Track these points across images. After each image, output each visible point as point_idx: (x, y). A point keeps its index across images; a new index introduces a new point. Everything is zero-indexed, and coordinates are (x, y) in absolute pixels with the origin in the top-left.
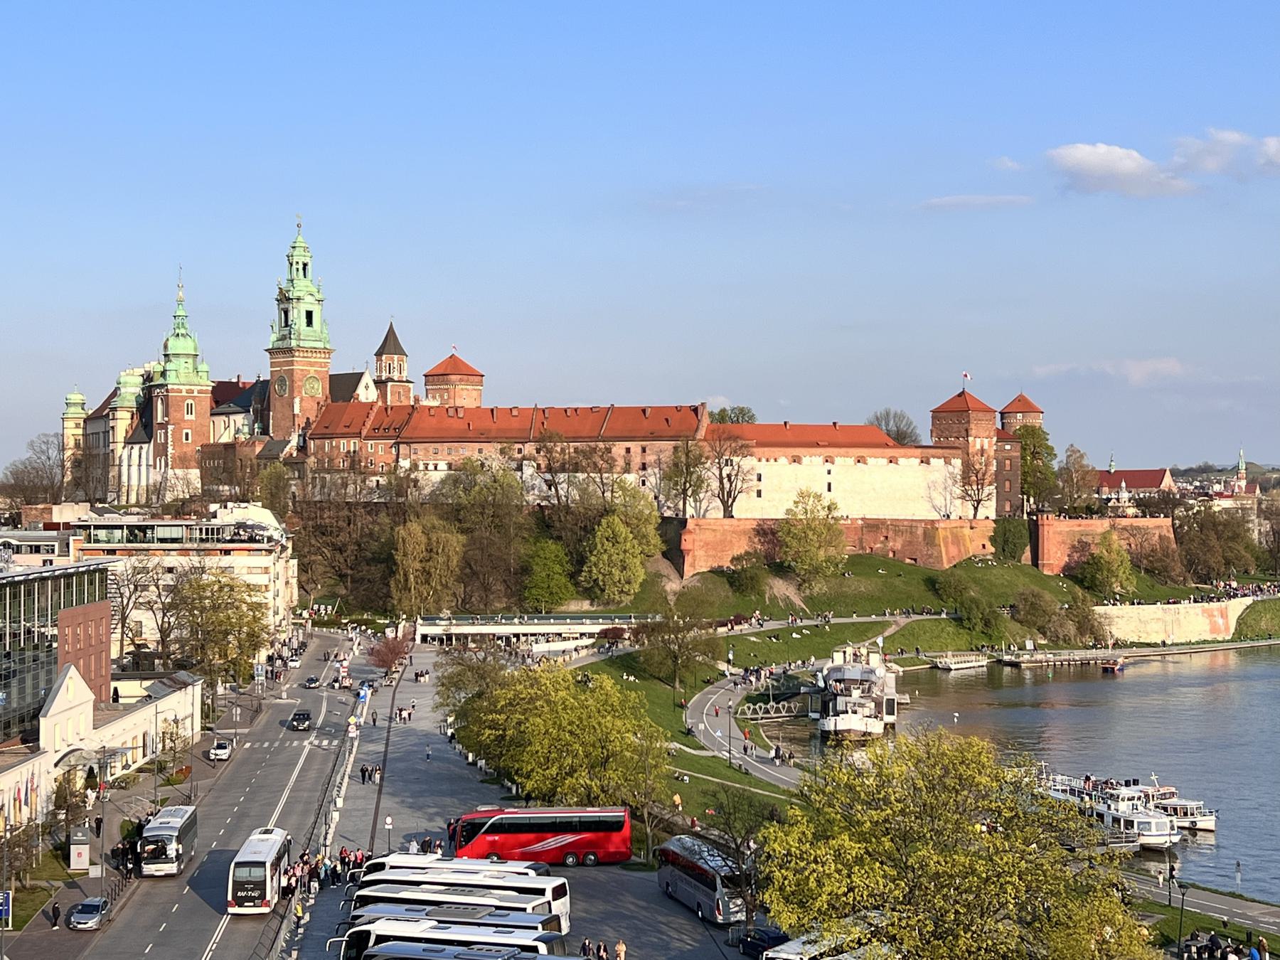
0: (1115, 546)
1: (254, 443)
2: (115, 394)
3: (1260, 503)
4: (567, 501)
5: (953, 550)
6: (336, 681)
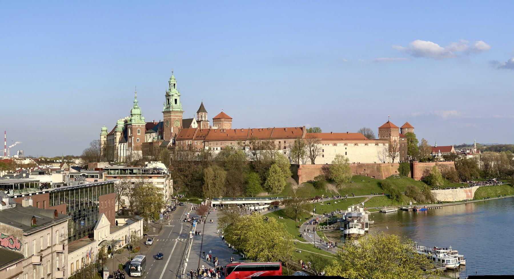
0: (437, 171)
1: (159, 142)
2: (116, 127)
3: (480, 156)
4: (260, 159)
5: (386, 173)
6: (186, 219)
